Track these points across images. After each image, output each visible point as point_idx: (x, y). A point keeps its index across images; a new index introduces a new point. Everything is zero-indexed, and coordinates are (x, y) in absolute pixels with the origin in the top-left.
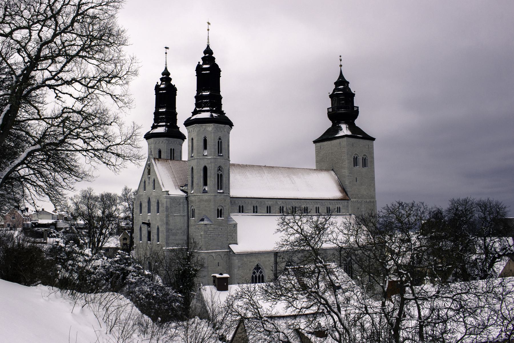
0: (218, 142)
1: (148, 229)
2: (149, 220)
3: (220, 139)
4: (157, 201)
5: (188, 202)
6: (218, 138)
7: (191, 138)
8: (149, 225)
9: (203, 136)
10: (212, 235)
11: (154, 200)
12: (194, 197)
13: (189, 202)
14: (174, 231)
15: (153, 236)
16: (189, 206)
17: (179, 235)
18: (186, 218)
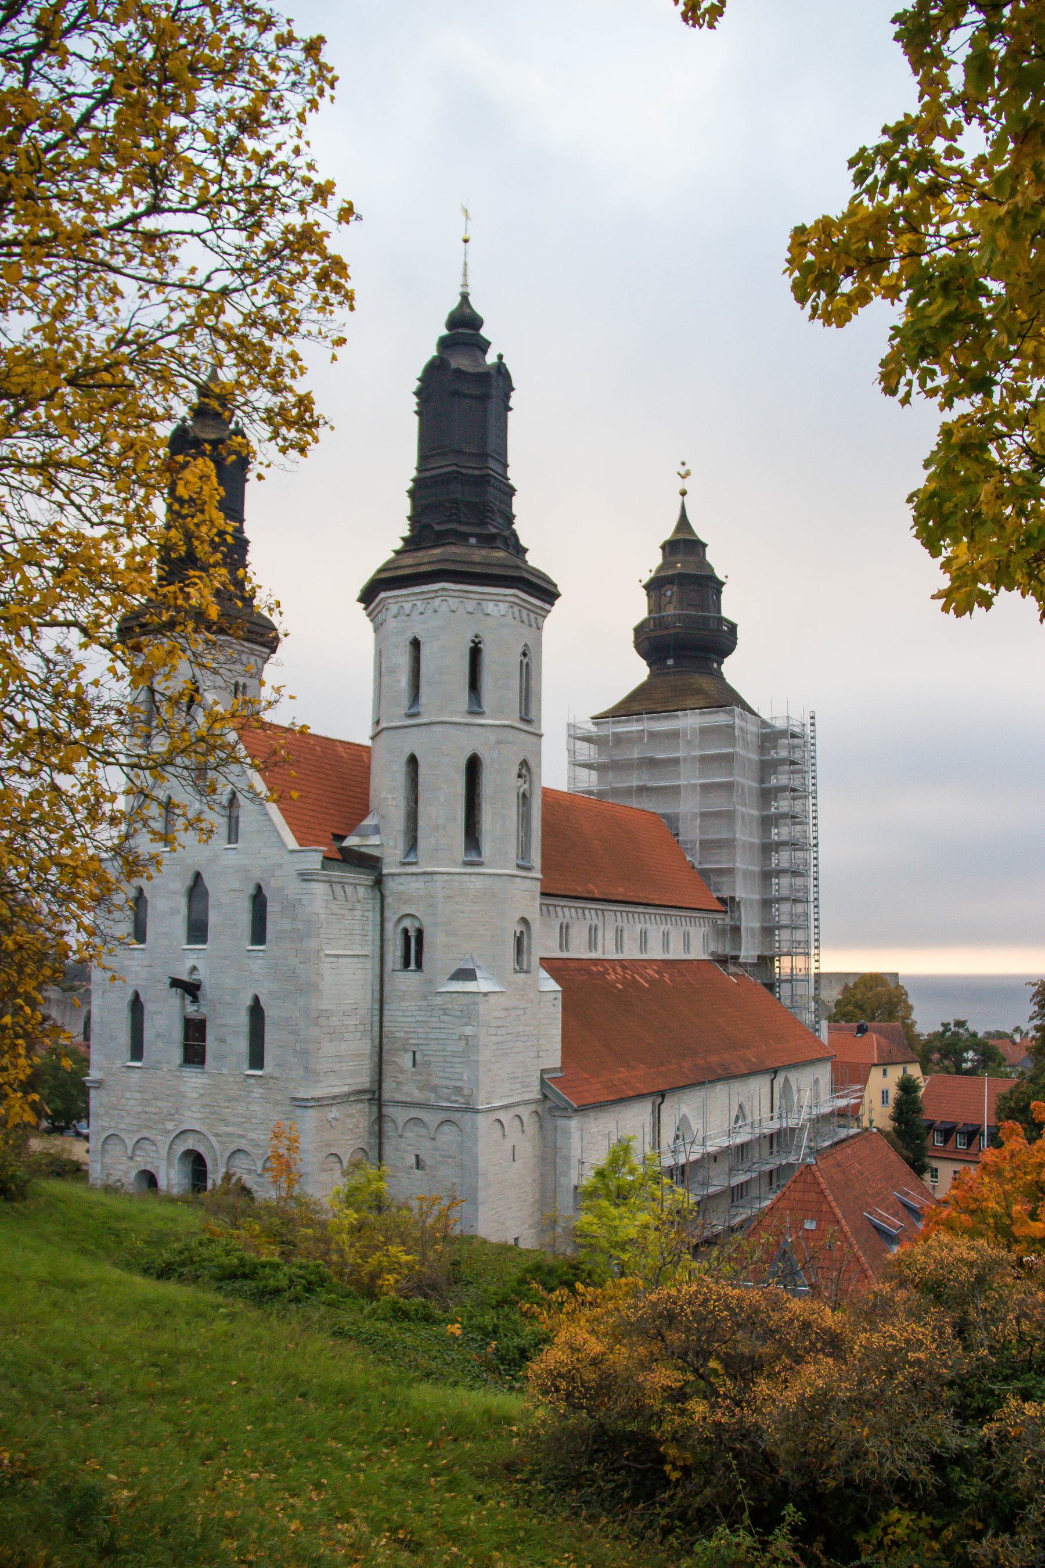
0: (521, 662)
1: (183, 1007)
2: (194, 968)
3: (524, 654)
4: (251, 890)
5: (383, 898)
6: (520, 650)
7: (409, 636)
8: (190, 989)
9: (469, 636)
10: (499, 1039)
11: (236, 885)
12: (421, 878)
13: (389, 900)
14: (334, 1021)
15: (223, 1041)
16: (388, 914)
17: (347, 1036)
18: (371, 966)
